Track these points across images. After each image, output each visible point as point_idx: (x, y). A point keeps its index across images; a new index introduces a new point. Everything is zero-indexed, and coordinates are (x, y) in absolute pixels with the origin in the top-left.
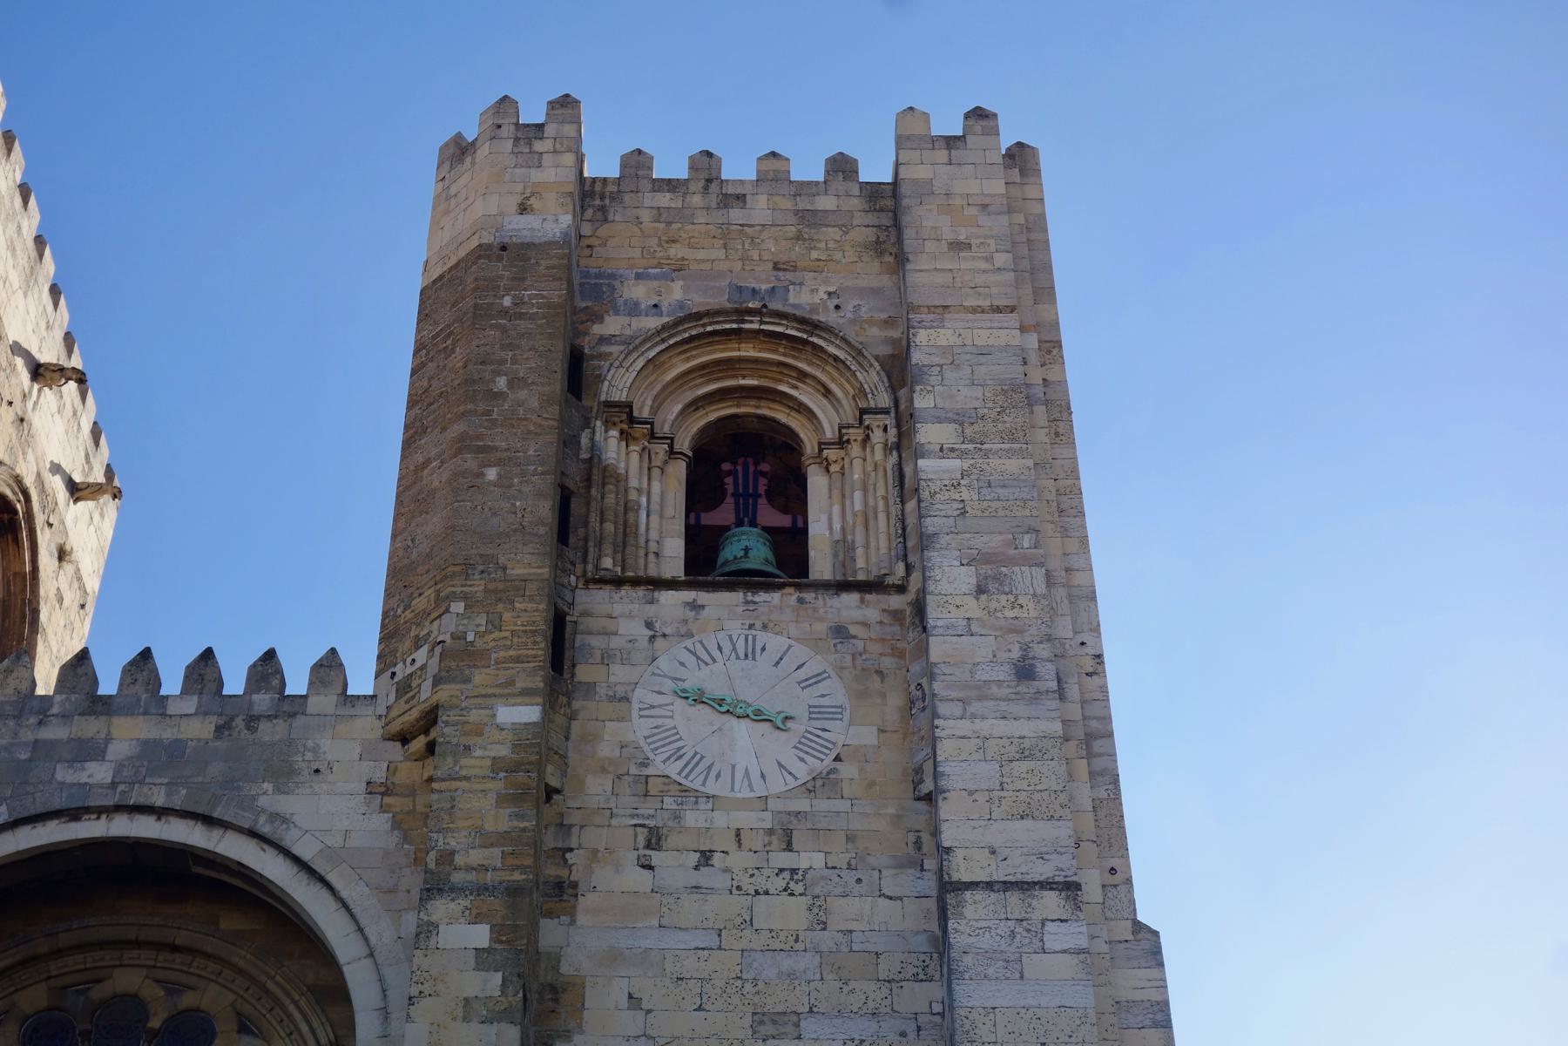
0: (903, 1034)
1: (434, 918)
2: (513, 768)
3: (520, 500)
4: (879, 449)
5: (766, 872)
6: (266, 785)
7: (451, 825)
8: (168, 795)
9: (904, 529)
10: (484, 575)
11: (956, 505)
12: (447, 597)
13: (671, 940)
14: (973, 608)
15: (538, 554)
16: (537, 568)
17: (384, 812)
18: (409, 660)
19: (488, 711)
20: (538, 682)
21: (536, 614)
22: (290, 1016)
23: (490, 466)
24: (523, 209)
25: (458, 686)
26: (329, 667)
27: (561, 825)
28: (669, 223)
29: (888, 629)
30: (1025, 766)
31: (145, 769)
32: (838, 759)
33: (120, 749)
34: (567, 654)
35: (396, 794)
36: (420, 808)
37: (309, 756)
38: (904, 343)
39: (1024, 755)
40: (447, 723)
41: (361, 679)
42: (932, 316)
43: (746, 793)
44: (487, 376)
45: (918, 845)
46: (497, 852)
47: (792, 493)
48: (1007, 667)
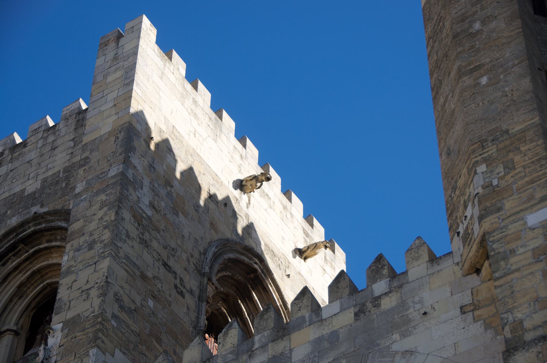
3: (508, 86)
6: (394, 336)
7: (515, 305)
10: (494, 142)
15: (529, 112)
16: (530, 120)
17: (476, 321)
19: (521, 222)
21: (537, 148)
23: (482, 76)
25: (495, 216)
31: (317, 358)
35: (482, 307)
37: (418, 306)
40: (494, 242)
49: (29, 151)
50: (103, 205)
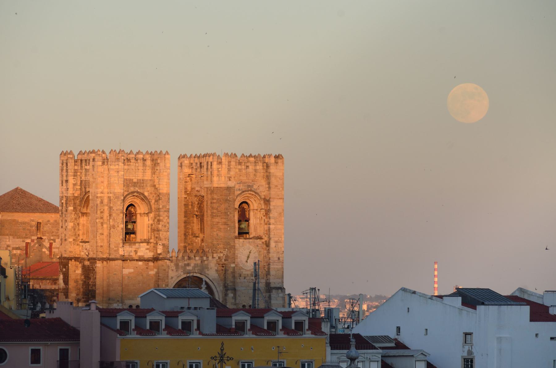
4: (262, 214)
8: (198, 271)
11: (274, 233)
12: (225, 248)
18: (220, 254)
24: (230, 180)
33: (192, 265)
39: (278, 271)
43: (248, 269)
45: (264, 275)
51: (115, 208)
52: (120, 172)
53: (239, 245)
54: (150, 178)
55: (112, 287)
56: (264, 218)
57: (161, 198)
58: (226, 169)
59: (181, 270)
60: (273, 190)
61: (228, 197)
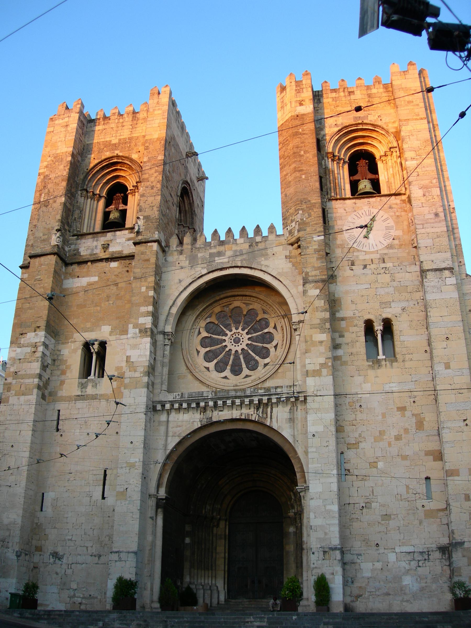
0: (414, 305)
1: (306, 289)
2: (319, 251)
4: (395, 157)
5: (379, 269)
8: (241, 263)
9: (404, 178)
13: (360, 287)
14: (423, 200)
20: (322, 229)
22: (274, 309)
24: (301, 104)
26: (272, 228)
27: (331, 261)
28: (336, 101)
29: (402, 205)
30: (437, 240)
32: (393, 239)
33: (229, 253)
34: (326, 219)
36: (298, 261)
37: (271, 251)
38: (399, 128)
39: (438, 237)
41: (280, 231)
42: (405, 122)
43: (372, 250)
44: (299, 151)
46: (318, 272)
47: (373, 169)
48: (432, 214)
49: (112, 123)
50: (156, 171)
51: (52, 176)
52: (71, 126)
53: (345, 210)
54: (143, 134)
55: (29, 303)
56: (399, 160)
57: (148, 147)
58: (294, 92)
59: (203, 265)
60: (402, 109)
61: (299, 129)
